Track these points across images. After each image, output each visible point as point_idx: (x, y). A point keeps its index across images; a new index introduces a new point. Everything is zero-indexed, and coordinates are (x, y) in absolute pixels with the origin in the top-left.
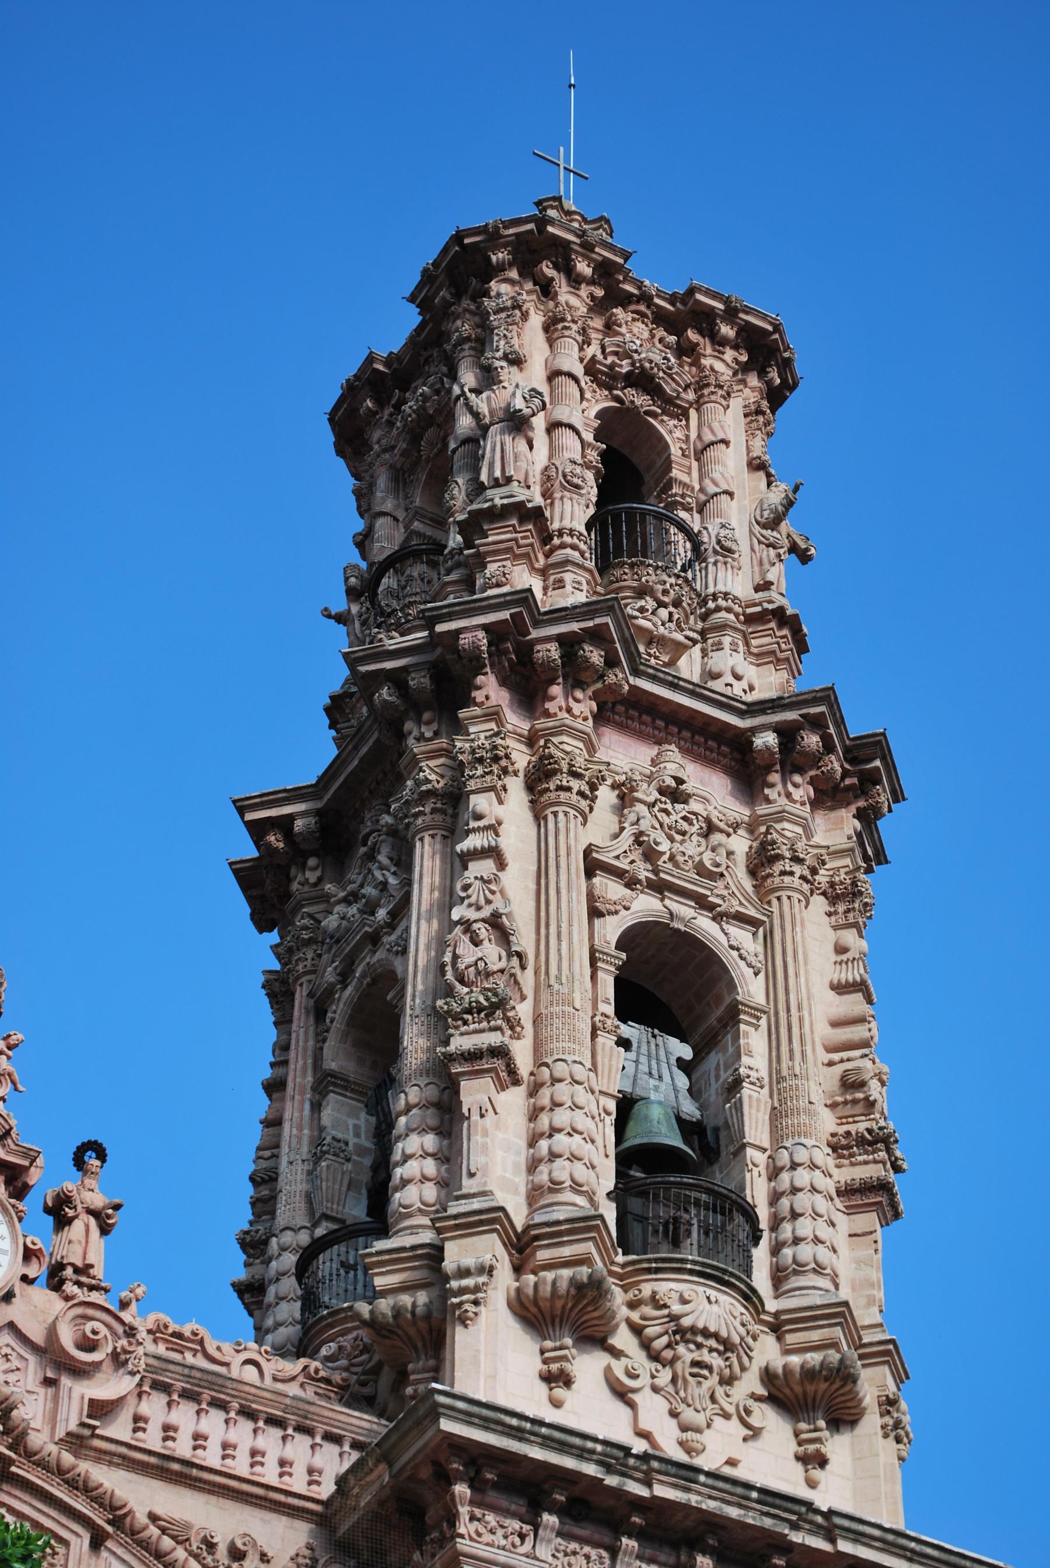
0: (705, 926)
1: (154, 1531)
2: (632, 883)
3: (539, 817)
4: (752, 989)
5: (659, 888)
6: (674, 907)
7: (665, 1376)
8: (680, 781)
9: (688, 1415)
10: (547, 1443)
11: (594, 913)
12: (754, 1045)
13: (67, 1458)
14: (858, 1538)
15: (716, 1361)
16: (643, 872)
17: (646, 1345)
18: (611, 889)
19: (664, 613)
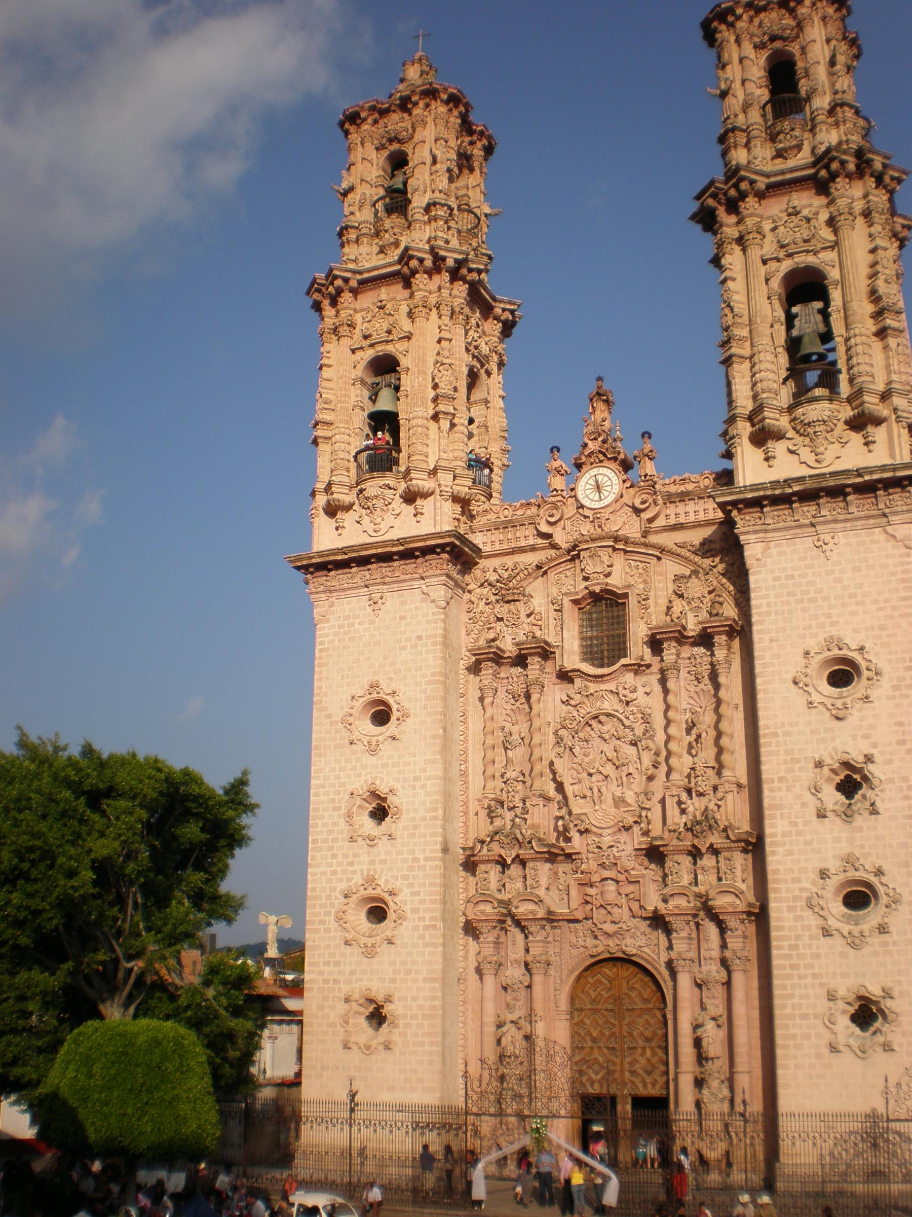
0: (811, 260)
1: (675, 548)
2: (778, 260)
3: (744, 253)
4: (834, 274)
5: (790, 255)
6: (796, 260)
7: (807, 440)
8: (794, 208)
9: (818, 450)
10: (752, 491)
11: (767, 280)
12: (836, 295)
13: (642, 540)
14: (871, 473)
15: (823, 428)
16: (782, 254)
17: (797, 432)
18: (773, 265)
19: (788, 137)
